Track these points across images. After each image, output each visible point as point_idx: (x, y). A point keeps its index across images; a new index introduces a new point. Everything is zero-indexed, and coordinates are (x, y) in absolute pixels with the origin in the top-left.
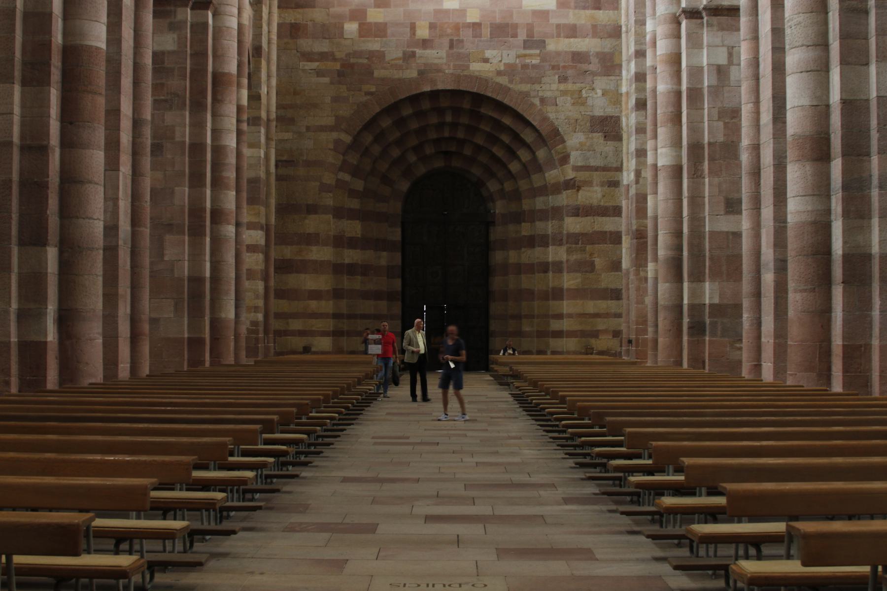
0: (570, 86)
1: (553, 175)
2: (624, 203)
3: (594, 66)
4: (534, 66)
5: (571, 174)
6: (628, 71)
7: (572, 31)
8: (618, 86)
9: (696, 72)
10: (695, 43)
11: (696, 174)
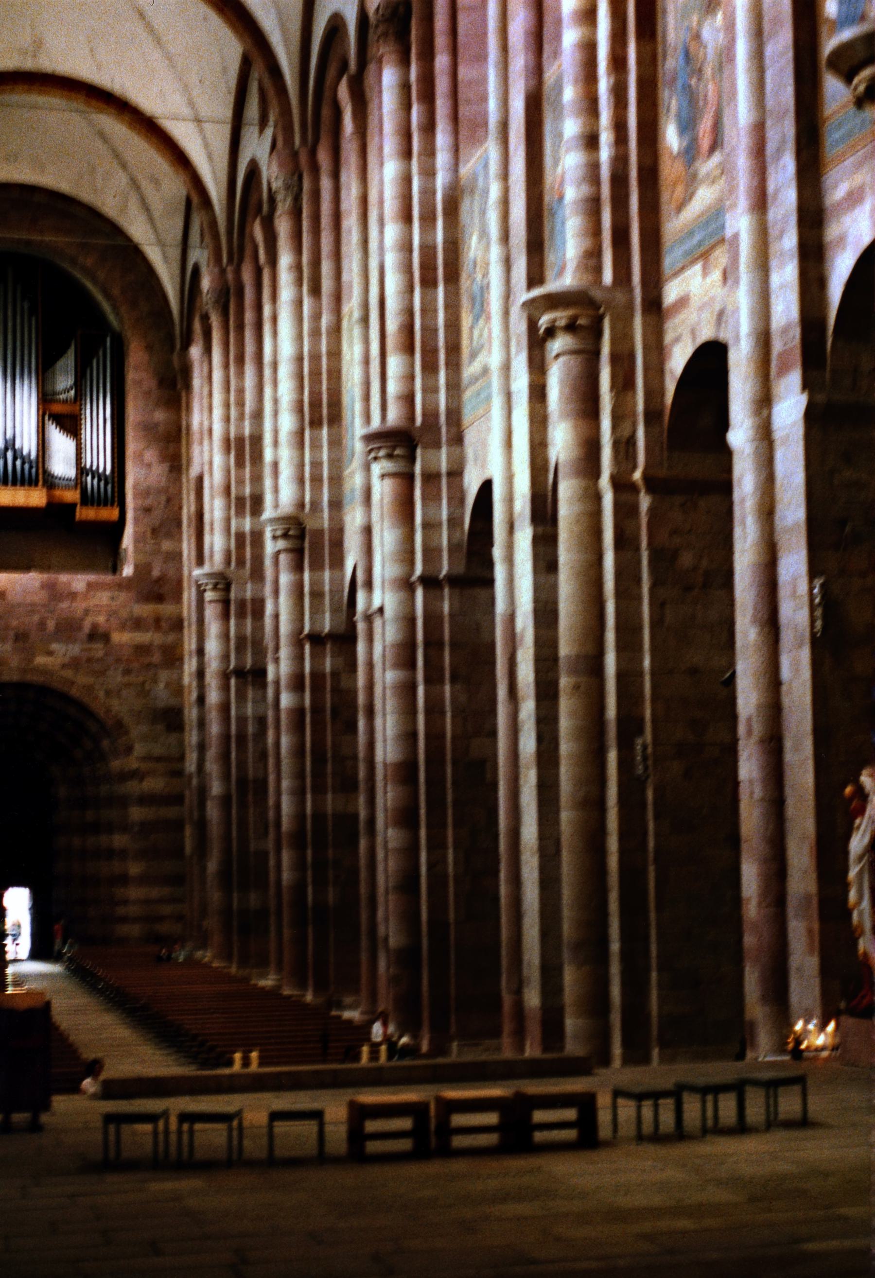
0: (132, 678)
1: (116, 764)
2: (187, 793)
3: (156, 658)
4: (99, 660)
5: (135, 765)
6: (190, 664)
7: (138, 624)
8: (180, 678)
9: (242, 720)
10: (241, 697)
11: (243, 805)
